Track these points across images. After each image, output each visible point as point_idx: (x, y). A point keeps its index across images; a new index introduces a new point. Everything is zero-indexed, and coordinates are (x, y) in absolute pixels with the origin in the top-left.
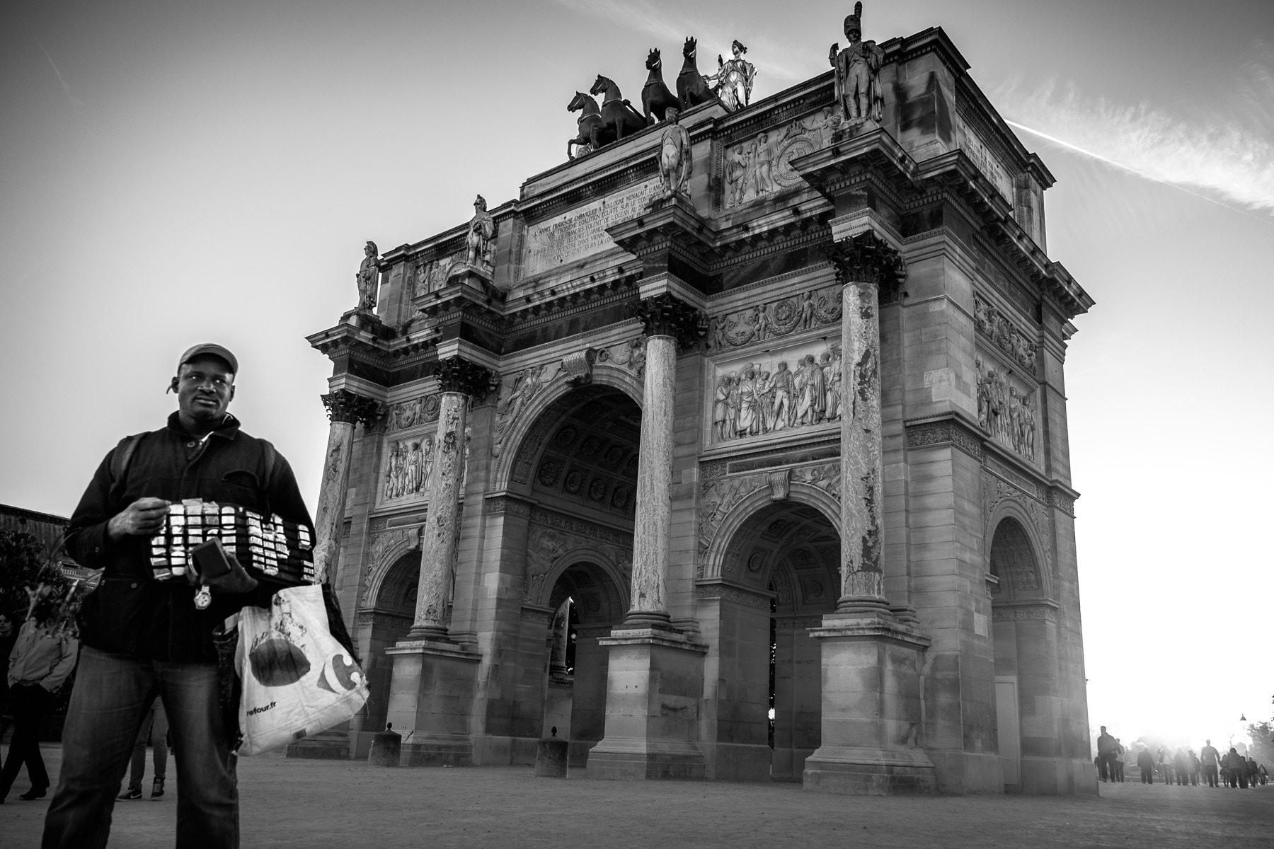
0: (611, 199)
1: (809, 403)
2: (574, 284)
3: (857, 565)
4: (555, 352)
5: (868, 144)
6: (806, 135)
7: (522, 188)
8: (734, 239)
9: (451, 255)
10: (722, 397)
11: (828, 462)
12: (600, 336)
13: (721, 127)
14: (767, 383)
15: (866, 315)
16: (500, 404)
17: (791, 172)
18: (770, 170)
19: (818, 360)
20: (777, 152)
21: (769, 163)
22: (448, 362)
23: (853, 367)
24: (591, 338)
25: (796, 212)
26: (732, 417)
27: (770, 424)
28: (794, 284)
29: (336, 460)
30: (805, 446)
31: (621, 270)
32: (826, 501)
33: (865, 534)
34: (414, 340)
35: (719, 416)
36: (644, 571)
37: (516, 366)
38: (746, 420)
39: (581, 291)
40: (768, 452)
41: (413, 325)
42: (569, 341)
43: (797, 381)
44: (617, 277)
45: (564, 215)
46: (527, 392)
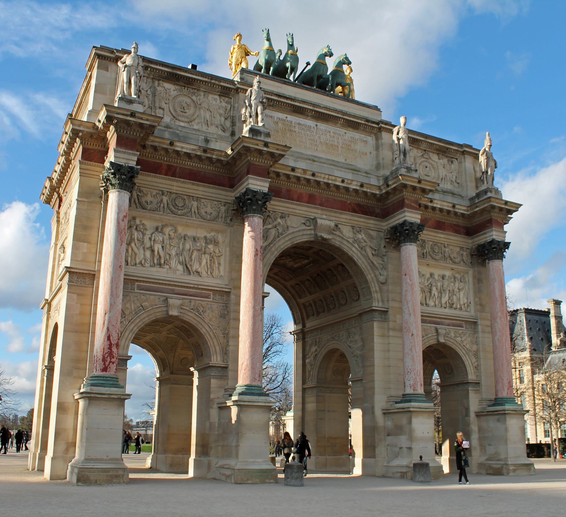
0: (322, 126)
1: (448, 299)
2: (330, 177)
4: (299, 210)
6: (430, 161)
8: (424, 203)
19: (447, 278)
25: (454, 206)
27: (428, 302)
30: (450, 319)
31: (362, 186)
32: (460, 347)
39: (332, 184)
40: (434, 317)
43: (439, 284)
44: (358, 188)
45: (286, 115)
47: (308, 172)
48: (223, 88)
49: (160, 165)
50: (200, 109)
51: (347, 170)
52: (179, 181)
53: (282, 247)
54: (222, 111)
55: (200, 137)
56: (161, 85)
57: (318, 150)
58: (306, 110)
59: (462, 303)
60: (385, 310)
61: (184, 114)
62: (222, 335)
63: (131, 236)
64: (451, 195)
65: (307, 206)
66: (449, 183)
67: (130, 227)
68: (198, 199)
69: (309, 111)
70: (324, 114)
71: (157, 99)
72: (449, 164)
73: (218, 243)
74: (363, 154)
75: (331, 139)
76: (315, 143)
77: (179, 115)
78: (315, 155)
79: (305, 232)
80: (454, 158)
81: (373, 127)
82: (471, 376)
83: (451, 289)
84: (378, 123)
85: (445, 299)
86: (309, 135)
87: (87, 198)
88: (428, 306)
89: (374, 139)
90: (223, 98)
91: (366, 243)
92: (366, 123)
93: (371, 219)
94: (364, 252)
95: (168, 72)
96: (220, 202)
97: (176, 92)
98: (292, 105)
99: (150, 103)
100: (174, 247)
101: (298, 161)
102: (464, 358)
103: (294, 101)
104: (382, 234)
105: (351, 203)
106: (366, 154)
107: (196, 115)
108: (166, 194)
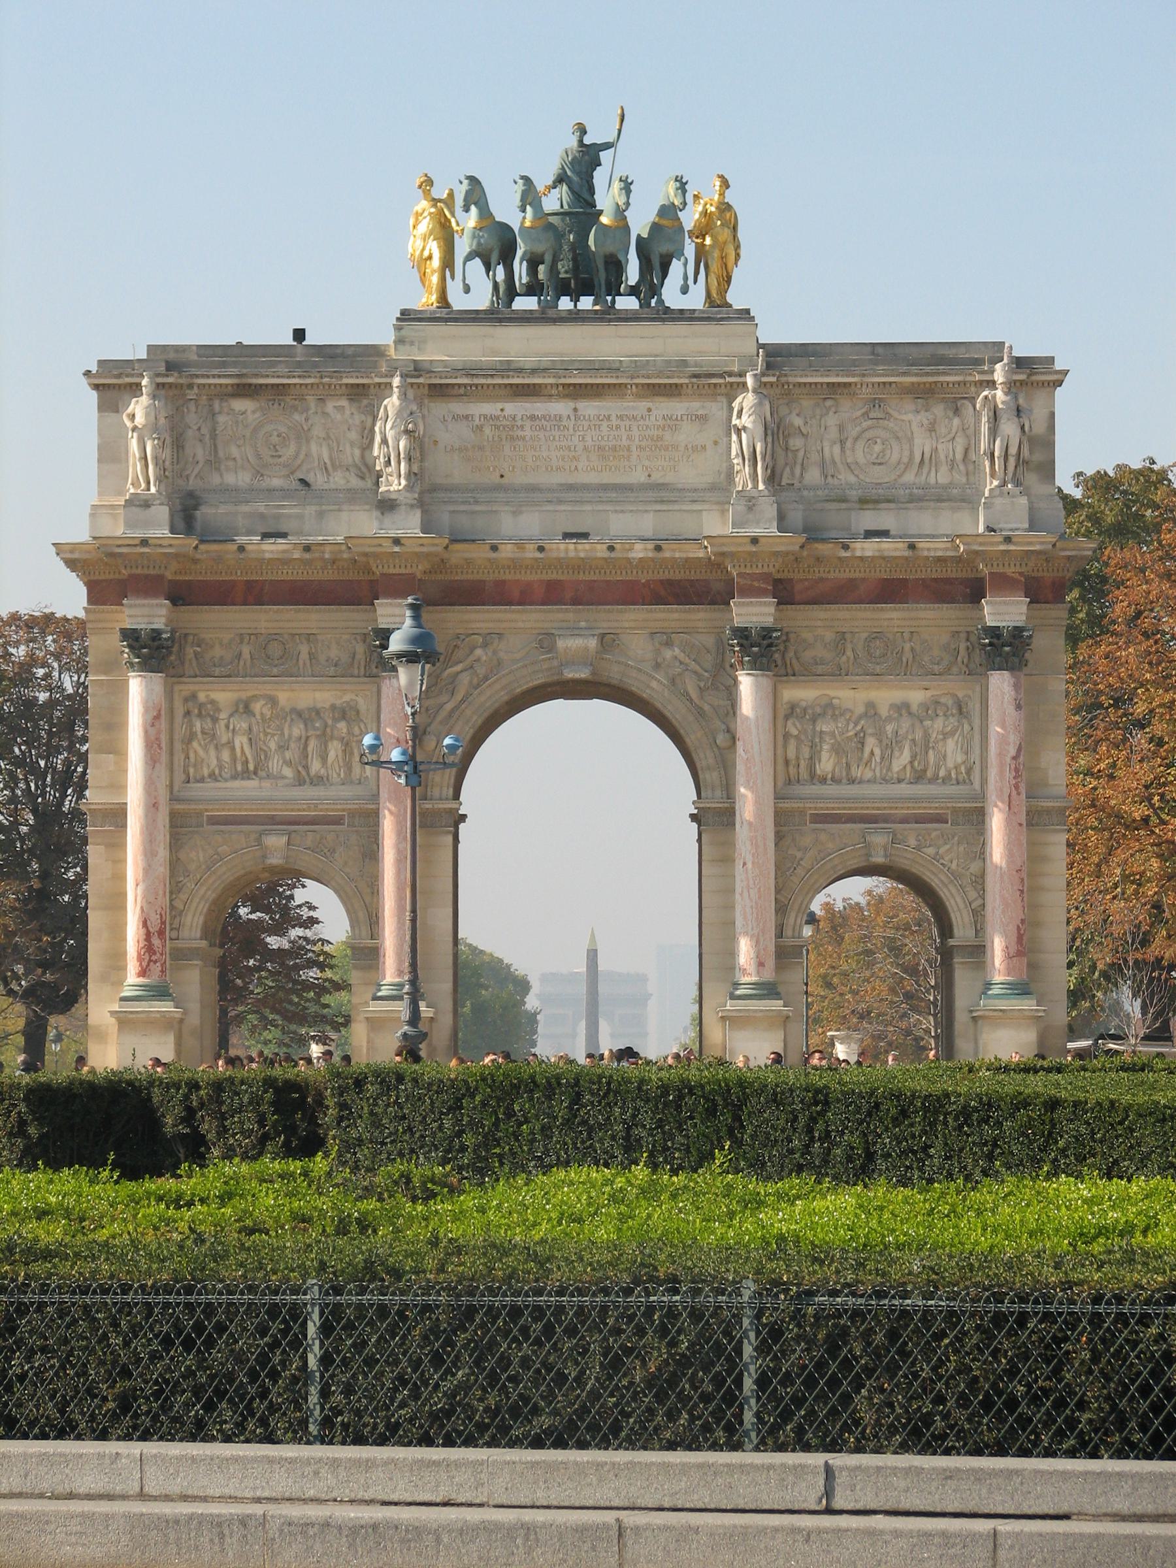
0: (589, 408)
1: (908, 759)
2: (580, 547)
3: (1012, 951)
5: (1042, 543)
6: (891, 425)
7: (398, 329)
10: (795, 732)
11: (936, 830)
13: (783, 379)
14: (851, 726)
15: (1018, 707)
19: (914, 708)
21: (842, 443)
23: (1008, 760)
25: (912, 547)
26: (807, 756)
29: (159, 732)
31: (658, 548)
33: (1019, 922)
35: (791, 754)
36: (762, 939)
38: (827, 764)
42: (549, 611)
43: (889, 728)
44: (650, 555)
45: (499, 406)
46: (481, 671)
49: (233, 584)
50: (308, 441)
53: (488, 705)
54: (353, 435)
56: (226, 410)
57: (580, 468)
59: (950, 764)
60: (726, 805)
62: (369, 890)
63: (191, 730)
64: (932, 504)
65: (540, 611)
66: (944, 469)
67: (188, 713)
68: (309, 637)
70: (586, 385)
72: (948, 417)
73: (358, 712)
74: (695, 449)
75: (612, 433)
81: (715, 385)
82: (962, 932)
83: (919, 735)
84: (721, 376)
85: (902, 759)
87: (105, 673)
88: (853, 782)
92: (694, 380)
95: (232, 385)
97: (258, 415)
98: (506, 385)
100: (273, 735)
101: (521, 512)
102: (944, 893)
105: (648, 581)
106: (704, 448)
107: (302, 457)
108: (246, 640)
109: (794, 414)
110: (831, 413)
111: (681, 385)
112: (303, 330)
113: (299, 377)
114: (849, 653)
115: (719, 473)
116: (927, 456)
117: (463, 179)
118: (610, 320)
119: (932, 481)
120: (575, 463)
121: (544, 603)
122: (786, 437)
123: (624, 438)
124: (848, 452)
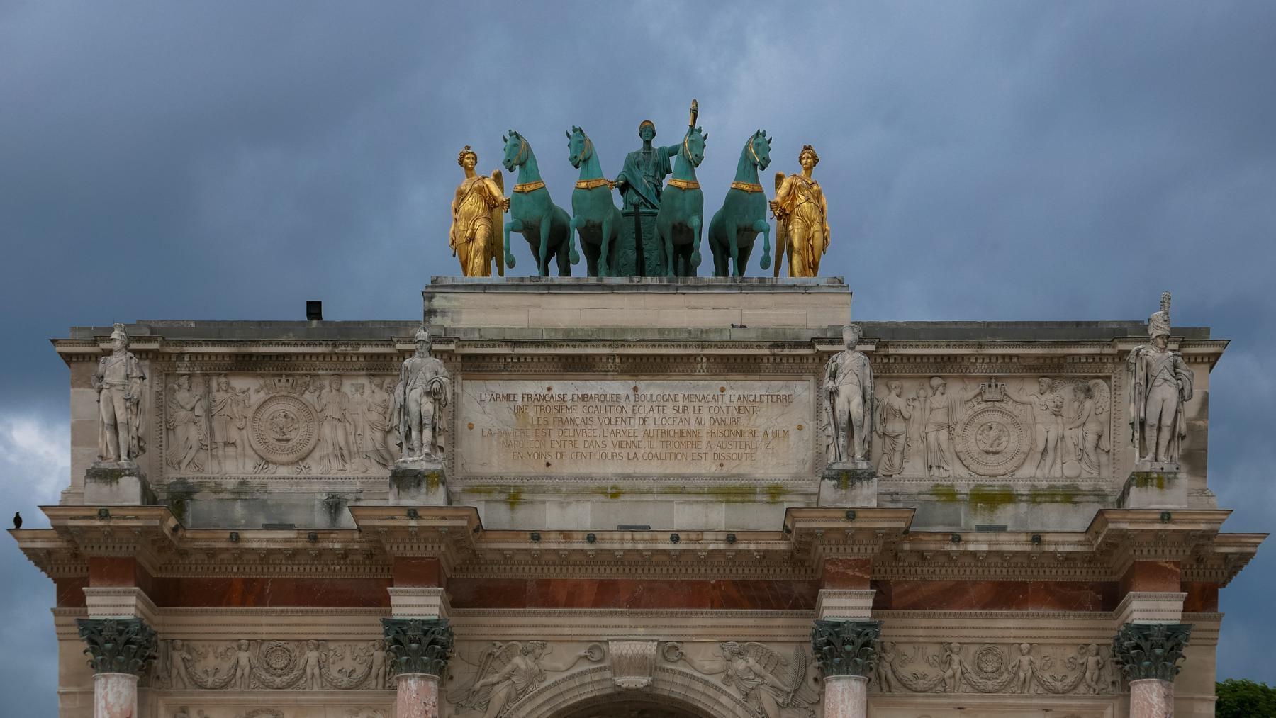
0: (652, 388)
2: (638, 536)
6: (1009, 406)
7: (429, 297)
9: (262, 376)
12: (666, 621)
13: (883, 351)
16: (451, 686)
17: (985, 456)
18: (951, 439)
20: (962, 415)
21: (950, 428)
22: (427, 627)
24: (652, 622)
28: (1008, 628)
31: (731, 539)
34: (248, 540)
37: (485, 630)
41: (196, 496)
42: (603, 615)
44: (722, 546)
45: (546, 384)
46: (520, 682)
47: (575, 536)
48: (368, 358)
50: (321, 422)
51: (710, 498)
52: (272, 611)
54: (375, 417)
55: (318, 496)
56: (223, 386)
57: (639, 455)
58: (597, 359)
61: (282, 444)
66: (1071, 459)
69: (604, 360)
70: (648, 356)
71: (216, 424)
72: (1077, 399)
74: (776, 435)
75: (679, 416)
76: (632, 439)
77: (273, 451)
78: (629, 470)
79: (587, 679)
80: (1098, 377)
81: (801, 357)
86: (613, 421)
89: (812, 385)
90: (377, 380)
91: (762, 677)
92: (776, 351)
93: (778, 616)
94: (753, 705)
95: (230, 355)
96: (371, 643)
98: (553, 356)
99: (202, 436)
101: (569, 503)
103: (556, 346)
104: (809, 649)
106: (786, 433)
107: (313, 441)
109: (894, 393)
110: (938, 393)
111: (761, 357)
112: (319, 304)
113: (309, 345)
114: (955, 666)
115: (804, 462)
116: (1051, 444)
117: (508, 137)
118: (677, 288)
119: (1058, 474)
120: (634, 449)
121: (595, 605)
122: (883, 421)
123: (693, 422)
124: (958, 440)
